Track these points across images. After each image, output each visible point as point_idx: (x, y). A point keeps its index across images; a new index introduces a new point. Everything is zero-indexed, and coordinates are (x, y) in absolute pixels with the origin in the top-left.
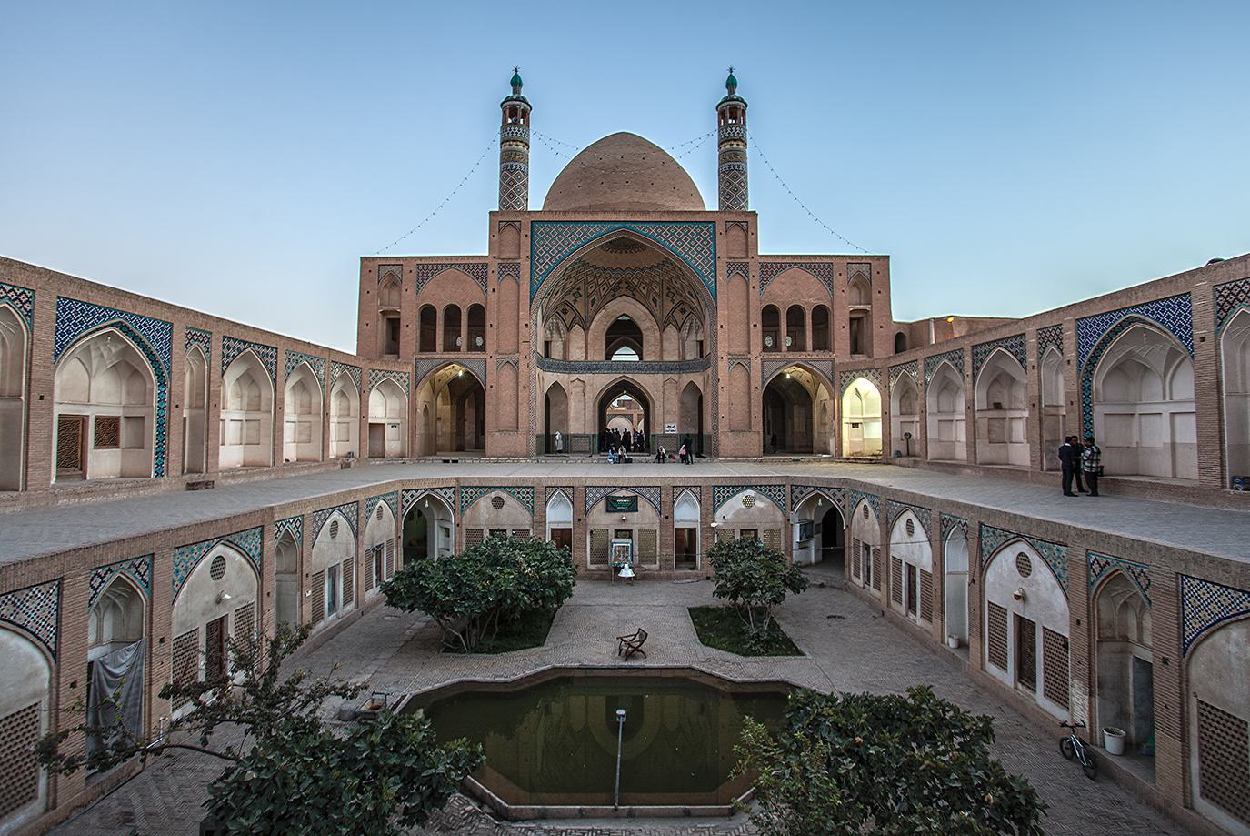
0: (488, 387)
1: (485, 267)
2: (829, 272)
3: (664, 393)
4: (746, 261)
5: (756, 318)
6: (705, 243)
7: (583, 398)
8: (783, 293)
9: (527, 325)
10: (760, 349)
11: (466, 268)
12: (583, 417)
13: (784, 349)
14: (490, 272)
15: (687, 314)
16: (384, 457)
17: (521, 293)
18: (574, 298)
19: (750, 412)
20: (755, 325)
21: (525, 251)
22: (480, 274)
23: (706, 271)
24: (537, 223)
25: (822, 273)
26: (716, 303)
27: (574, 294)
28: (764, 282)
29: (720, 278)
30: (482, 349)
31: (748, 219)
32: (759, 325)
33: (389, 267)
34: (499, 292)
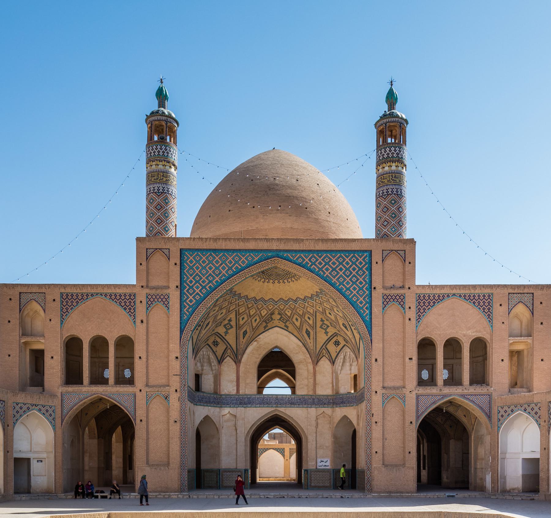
0: (138, 421)
1: (132, 297)
2: (489, 303)
3: (317, 427)
4: (401, 291)
5: (413, 351)
6: (361, 273)
7: (234, 433)
8: (441, 325)
9: (177, 358)
10: (415, 382)
11: (113, 297)
12: (235, 451)
13: (440, 382)
14: (138, 302)
15: (341, 346)
16: (29, 492)
17: (171, 325)
18: (225, 330)
19: (404, 447)
20: (411, 359)
21: (175, 281)
22: (128, 304)
23: (361, 303)
24: (186, 253)
25: (482, 304)
26: (371, 335)
27: (225, 326)
28: (420, 314)
29: (375, 310)
30: (131, 382)
31: (407, 248)
32: (415, 358)
33: (30, 295)
34: (147, 323)
